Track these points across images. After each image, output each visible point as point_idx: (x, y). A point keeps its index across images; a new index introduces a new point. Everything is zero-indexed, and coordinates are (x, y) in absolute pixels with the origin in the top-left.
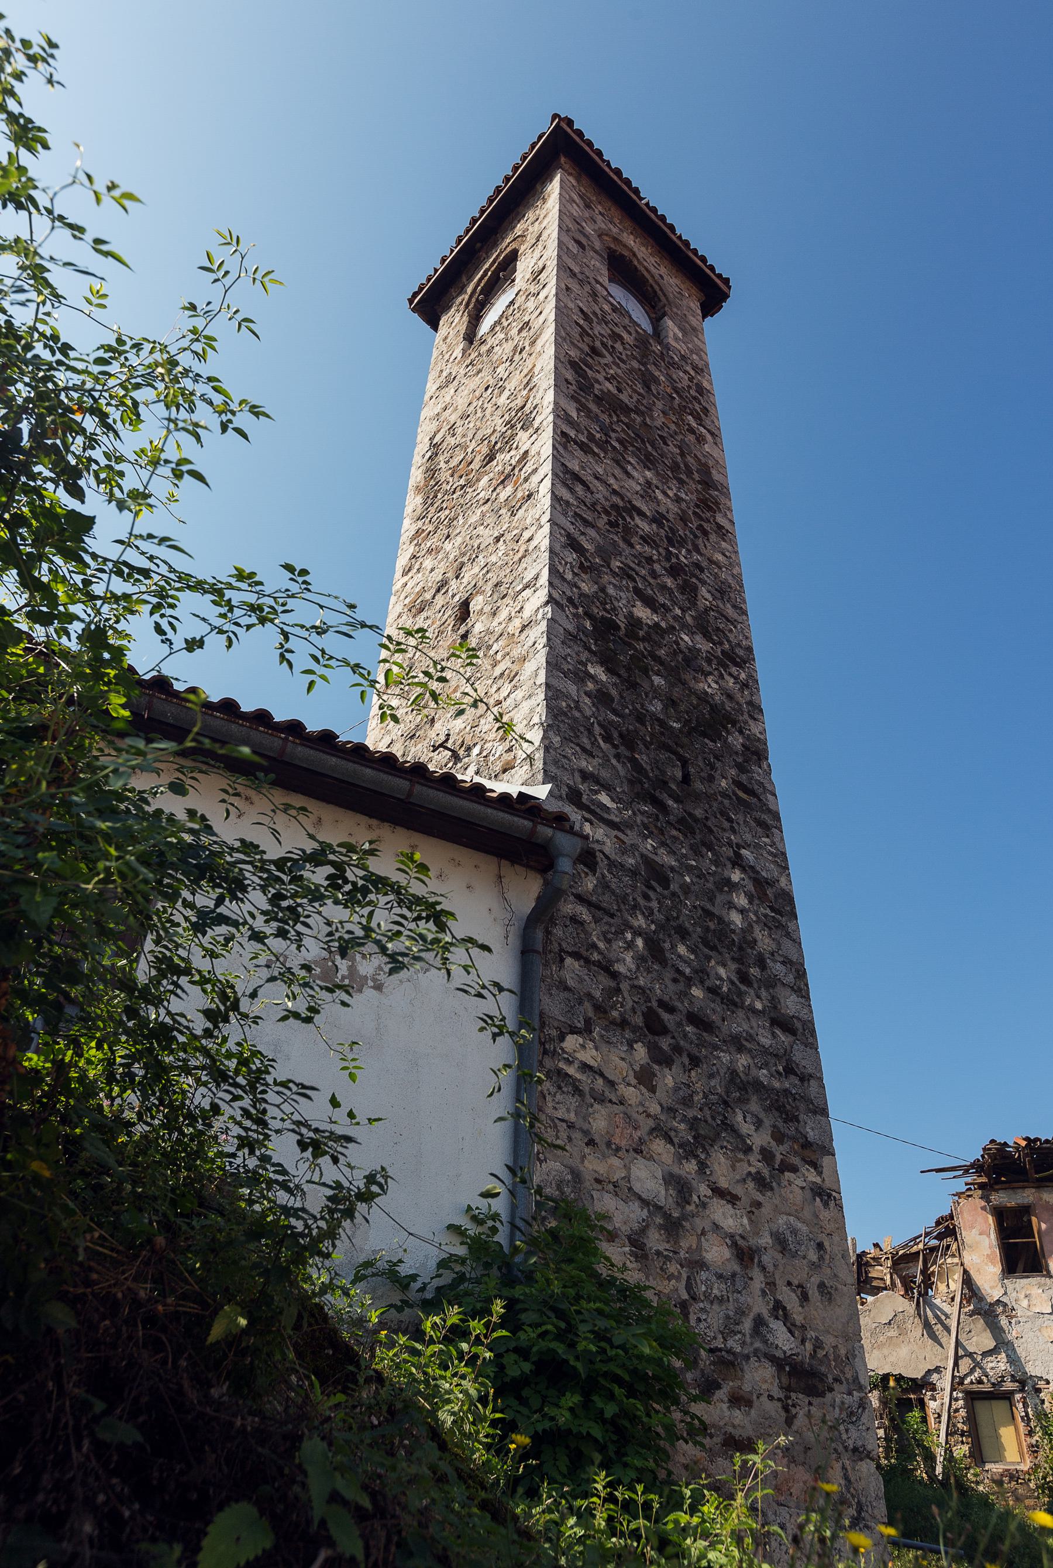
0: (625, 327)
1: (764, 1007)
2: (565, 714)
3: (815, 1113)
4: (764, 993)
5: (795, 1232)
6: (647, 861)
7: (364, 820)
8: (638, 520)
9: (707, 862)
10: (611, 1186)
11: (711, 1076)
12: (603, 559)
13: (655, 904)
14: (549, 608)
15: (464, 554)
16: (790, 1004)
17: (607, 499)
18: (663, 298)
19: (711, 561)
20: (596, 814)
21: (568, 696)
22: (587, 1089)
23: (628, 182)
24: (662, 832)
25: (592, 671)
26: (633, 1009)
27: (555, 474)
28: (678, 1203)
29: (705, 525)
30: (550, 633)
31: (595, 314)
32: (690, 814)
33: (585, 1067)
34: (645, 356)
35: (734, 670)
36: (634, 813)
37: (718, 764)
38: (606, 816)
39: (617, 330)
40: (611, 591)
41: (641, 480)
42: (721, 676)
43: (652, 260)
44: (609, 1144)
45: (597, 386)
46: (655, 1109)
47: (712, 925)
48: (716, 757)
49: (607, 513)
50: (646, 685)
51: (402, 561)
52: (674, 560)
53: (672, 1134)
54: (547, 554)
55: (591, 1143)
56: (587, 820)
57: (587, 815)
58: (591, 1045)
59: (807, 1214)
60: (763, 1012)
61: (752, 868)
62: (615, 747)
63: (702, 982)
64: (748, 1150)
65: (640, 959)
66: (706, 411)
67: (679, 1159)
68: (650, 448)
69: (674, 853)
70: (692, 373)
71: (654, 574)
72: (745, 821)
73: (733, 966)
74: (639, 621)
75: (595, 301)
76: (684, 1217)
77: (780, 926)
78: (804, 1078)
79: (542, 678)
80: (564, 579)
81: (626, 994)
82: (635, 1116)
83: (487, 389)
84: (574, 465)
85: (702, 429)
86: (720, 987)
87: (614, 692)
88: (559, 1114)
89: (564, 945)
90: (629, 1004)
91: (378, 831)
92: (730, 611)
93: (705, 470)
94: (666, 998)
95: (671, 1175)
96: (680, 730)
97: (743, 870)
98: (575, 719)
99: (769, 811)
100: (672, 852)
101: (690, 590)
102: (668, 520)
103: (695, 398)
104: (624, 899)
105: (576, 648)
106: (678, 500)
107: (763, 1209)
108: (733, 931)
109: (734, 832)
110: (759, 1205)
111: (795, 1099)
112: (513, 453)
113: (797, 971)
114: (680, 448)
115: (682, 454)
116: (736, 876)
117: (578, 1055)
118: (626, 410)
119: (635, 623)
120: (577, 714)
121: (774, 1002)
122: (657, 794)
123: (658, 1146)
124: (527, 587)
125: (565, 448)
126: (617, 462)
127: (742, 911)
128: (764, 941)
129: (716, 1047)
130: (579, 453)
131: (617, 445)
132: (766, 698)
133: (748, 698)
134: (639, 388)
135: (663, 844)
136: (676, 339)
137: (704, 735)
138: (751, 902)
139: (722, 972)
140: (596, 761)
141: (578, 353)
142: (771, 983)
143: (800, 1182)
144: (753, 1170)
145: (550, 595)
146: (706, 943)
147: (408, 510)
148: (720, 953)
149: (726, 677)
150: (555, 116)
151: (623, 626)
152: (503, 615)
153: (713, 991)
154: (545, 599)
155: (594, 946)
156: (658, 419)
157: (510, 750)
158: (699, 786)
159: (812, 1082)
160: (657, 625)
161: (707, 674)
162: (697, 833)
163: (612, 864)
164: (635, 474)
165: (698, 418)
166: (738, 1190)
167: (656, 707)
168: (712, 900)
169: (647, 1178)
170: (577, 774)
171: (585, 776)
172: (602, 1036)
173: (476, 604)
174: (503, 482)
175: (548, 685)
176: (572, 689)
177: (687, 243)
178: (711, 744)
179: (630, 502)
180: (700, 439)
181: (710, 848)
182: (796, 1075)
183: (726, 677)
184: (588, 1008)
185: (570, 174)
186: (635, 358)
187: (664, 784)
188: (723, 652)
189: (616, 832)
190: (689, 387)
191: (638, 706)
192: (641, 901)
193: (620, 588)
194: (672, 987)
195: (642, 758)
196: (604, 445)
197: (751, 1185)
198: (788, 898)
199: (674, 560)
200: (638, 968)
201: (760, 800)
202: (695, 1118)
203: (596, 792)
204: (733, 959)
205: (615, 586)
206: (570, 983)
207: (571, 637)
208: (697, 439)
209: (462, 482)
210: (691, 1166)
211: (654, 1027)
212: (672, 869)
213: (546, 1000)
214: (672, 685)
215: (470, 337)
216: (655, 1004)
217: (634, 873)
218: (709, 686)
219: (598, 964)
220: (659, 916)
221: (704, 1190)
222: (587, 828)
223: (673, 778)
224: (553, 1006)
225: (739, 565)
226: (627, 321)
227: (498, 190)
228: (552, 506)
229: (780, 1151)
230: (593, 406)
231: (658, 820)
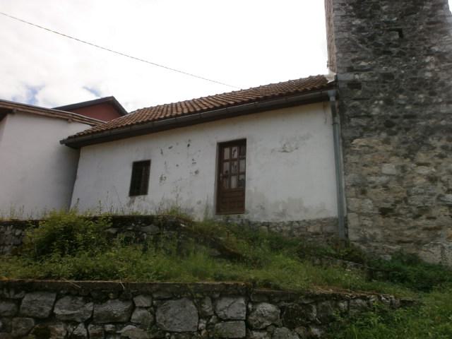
13: (388, 87)
20: (362, 70)
24: (389, 61)
25: (354, 23)
46: (390, 148)
61: (437, 52)
73: (428, 92)
87: (365, 25)
90: (378, 122)
95: (398, 166)
96: (397, 20)
97: (432, 55)
100: (394, 66)
104: (374, 92)
109: (426, 43)
110: (440, 163)
122: (387, 50)
139: (421, 96)
140: (358, 54)
144: (437, 154)
146: (412, 90)
153: (417, 104)
167: (385, 17)
168: (415, 73)
171: (353, 61)
176: (346, 35)
178: (414, 16)
184: (361, 130)
187: (389, 44)
192: (381, 89)
195: (380, 40)
204: (427, 89)
211: (389, 125)
212: (395, 72)
219: (364, 116)
220: (389, 90)
222: (357, 76)
223: (395, 40)
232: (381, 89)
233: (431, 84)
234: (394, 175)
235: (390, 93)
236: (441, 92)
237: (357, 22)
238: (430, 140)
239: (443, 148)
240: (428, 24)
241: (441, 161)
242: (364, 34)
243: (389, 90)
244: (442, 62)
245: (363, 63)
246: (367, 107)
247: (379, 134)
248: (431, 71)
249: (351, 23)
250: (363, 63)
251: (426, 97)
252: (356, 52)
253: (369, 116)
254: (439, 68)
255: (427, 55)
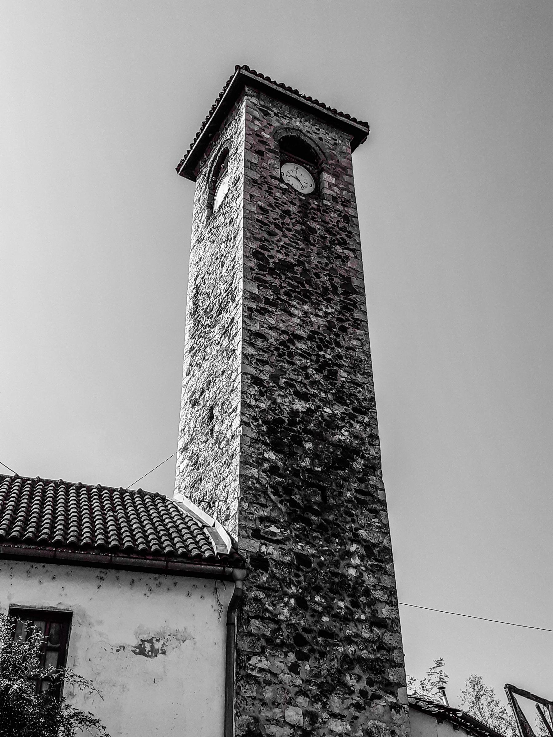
0: (291, 202)
1: (367, 618)
2: (250, 489)
3: (395, 667)
4: (367, 610)
5: (377, 728)
6: (298, 556)
7: (153, 576)
8: (298, 345)
9: (336, 547)
10: (275, 722)
11: (332, 660)
12: (274, 382)
13: (302, 578)
14: (241, 428)
15: (210, 375)
16: (385, 611)
17: (276, 340)
18: (322, 157)
19: (348, 348)
20: (269, 539)
21: (252, 477)
22: (262, 680)
23: (289, 89)
24: (307, 536)
25: (266, 456)
26: (288, 637)
27: (244, 340)
28: (310, 724)
29: (346, 324)
30: (241, 444)
31: (270, 205)
32: (326, 520)
33: (261, 670)
34: (305, 215)
35: (360, 418)
36: (291, 531)
37: (346, 484)
38: (274, 538)
39: (286, 208)
40: (279, 400)
41: (301, 315)
42: (351, 425)
43: (314, 128)
44: (273, 703)
45: (271, 261)
46: (299, 682)
47: (336, 580)
48: (345, 480)
49: (277, 349)
50: (300, 452)
51: (186, 365)
52: (322, 360)
53: (309, 692)
54: (240, 394)
55: (264, 704)
56: (263, 544)
57: (263, 541)
58: (264, 659)
59: (386, 718)
60: (366, 620)
61: (365, 540)
62: (280, 496)
63: (328, 613)
64: (353, 692)
65: (293, 610)
66: (350, 234)
67: (312, 703)
68: (307, 287)
69: (315, 546)
70: (341, 208)
71: (307, 376)
72: (362, 514)
73: (348, 599)
74: (297, 412)
75: (270, 194)
76: (313, 730)
77: (381, 568)
78: (391, 650)
79: (238, 473)
80: (250, 406)
81: (284, 630)
82: (288, 687)
83: (217, 259)
84: (256, 328)
85: (347, 252)
86: (339, 613)
87: (280, 464)
88: (248, 694)
89: (250, 614)
91: (159, 580)
92: (360, 378)
93: (347, 282)
94: (307, 626)
95: (307, 711)
96: (322, 471)
97: (358, 542)
98: (256, 489)
99: (379, 501)
100: (313, 546)
101: (332, 376)
102: (318, 333)
103: (341, 229)
104: (284, 580)
105: (257, 446)
106: (327, 314)
107: (359, 720)
108: (351, 580)
109: (353, 521)
110: (356, 718)
111: (383, 662)
112: (228, 314)
113: (390, 592)
114: (329, 275)
115: (331, 279)
116: (353, 548)
117: (257, 665)
118: (290, 267)
119: (294, 413)
120: (258, 486)
121: (374, 613)
123: (301, 699)
124: (233, 411)
125: (250, 318)
126: (284, 310)
127: (357, 567)
128: (369, 580)
129: (335, 645)
130: (258, 317)
131: (284, 298)
132: (383, 430)
133: (370, 433)
134: (302, 245)
135: (307, 543)
136: (330, 185)
137: (337, 468)
138: (362, 560)
139: (342, 604)
140: (268, 510)
141: (259, 243)
142: (372, 603)
143: (383, 703)
144: (354, 702)
145: (242, 421)
146: (331, 591)
147: (188, 328)
148: (341, 594)
149: (355, 424)
150: (237, 67)
151: (286, 420)
152: (226, 423)
154: (239, 423)
155: (267, 610)
156: (314, 259)
157: (228, 509)
158: (332, 501)
159: (396, 651)
160: (309, 409)
161: (340, 428)
162: (330, 531)
163: (278, 564)
164: (296, 312)
165: (343, 243)
166: (345, 713)
168: (337, 564)
169: (293, 715)
170: (257, 521)
171: (262, 519)
172: (270, 653)
173: (217, 411)
174: (224, 333)
175: (241, 476)
176: (254, 472)
177: (335, 111)
178: (341, 473)
179: (293, 334)
180: (344, 259)
181: (337, 536)
182: (384, 649)
183: (355, 424)
184: (263, 642)
185: (252, 96)
186: (298, 222)
187: (308, 508)
188: (353, 409)
189: (279, 546)
190: (339, 221)
191: (295, 466)
192: (294, 579)
193: (285, 397)
194: (310, 620)
195: (297, 498)
196: (273, 304)
197: (352, 709)
198: (388, 550)
199: (322, 360)
200: (291, 615)
201: (373, 496)
202: (322, 682)
203: (268, 527)
204: (349, 596)
205: (281, 396)
206: (254, 631)
207: (255, 441)
208: (343, 261)
209: (208, 322)
210: (319, 706)
212: (313, 555)
213: (240, 643)
214: (316, 445)
215: (210, 205)
216: (300, 631)
217: (289, 565)
218: (343, 436)
219: (269, 618)
220: (304, 584)
221: (325, 715)
222: (264, 548)
223: (316, 503)
224: (245, 646)
225: (368, 342)
226: (293, 195)
227: (214, 107)
228: (243, 363)
229: (371, 691)
230: (269, 278)
231: (305, 529)
232: (294, 579)
233: (354, 588)
234: (298, 727)
235: (305, 589)
236: (364, 604)
237: (271, 455)
238: (348, 678)
239: (363, 693)
240: (357, 491)
241: (357, 714)
242: (280, 479)
243: (304, 584)
244: (369, 557)
245: (273, 529)
246: (274, 605)
247: (286, 654)
248: (357, 567)
249: (262, 454)
250: (273, 529)
251: (347, 608)
252: (266, 506)
253: (274, 619)
254: (365, 566)
255: (352, 541)
